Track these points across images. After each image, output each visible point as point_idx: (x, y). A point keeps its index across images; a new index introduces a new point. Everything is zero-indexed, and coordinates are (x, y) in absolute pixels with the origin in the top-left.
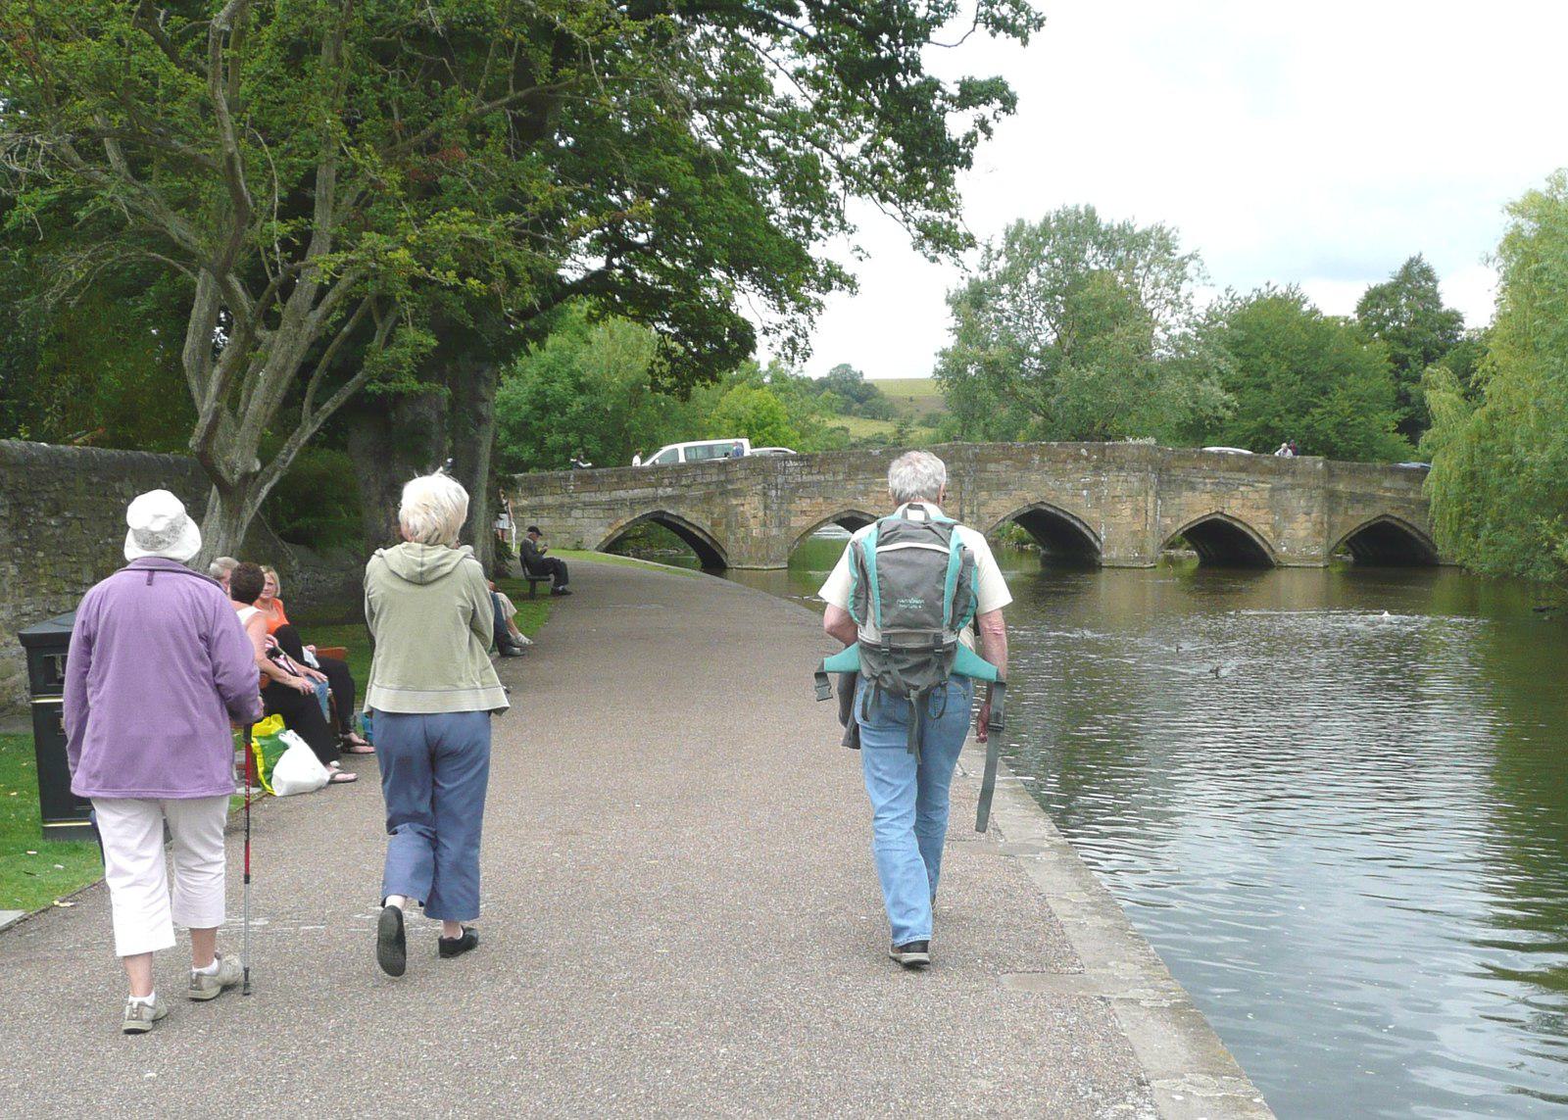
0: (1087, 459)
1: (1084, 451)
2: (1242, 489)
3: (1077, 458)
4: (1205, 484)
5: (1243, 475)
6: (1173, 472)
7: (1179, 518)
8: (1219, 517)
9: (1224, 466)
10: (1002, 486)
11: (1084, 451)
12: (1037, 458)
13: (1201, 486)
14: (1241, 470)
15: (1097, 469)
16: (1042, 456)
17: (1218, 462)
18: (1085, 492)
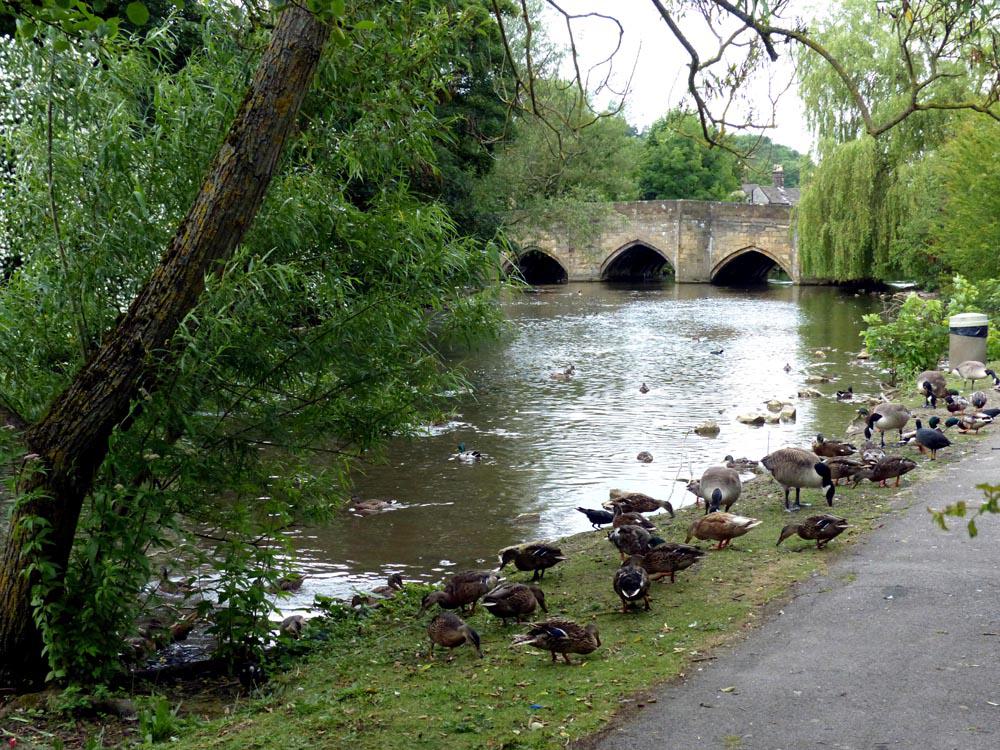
0: (665, 211)
1: (664, 207)
2: (767, 229)
3: (659, 211)
4: (742, 226)
5: (769, 220)
6: (721, 218)
7: (724, 251)
8: (754, 249)
9: (756, 213)
10: (614, 230)
11: (664, 207)
12: (635, 211)
13: (739, 228)
14: (768, 216)
15: (671, 219)
16: (638, 209)
17: (752, 211)
18: (664, 233)
